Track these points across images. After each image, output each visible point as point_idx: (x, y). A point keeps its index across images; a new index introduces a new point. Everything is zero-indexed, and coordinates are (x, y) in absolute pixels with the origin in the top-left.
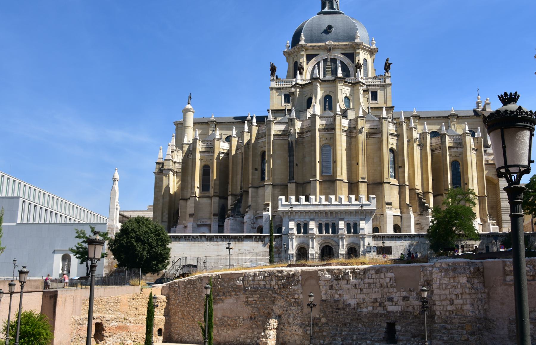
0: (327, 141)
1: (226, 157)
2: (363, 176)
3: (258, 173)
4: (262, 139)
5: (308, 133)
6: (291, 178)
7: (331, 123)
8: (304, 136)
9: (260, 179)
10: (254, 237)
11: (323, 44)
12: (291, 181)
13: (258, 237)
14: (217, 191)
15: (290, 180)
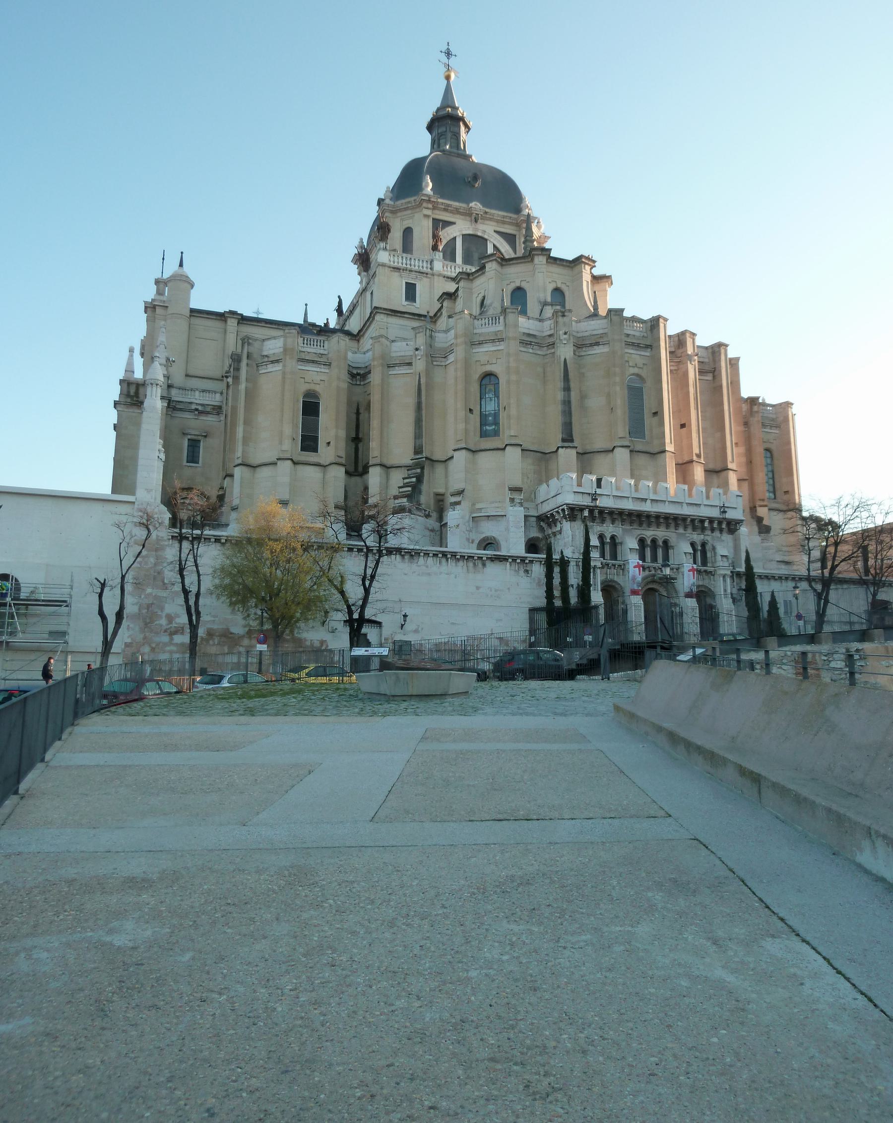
0: (636, 370)
1: (349, 380)
2: (698, 452)
3: (475, 418)
4: (485, 345)
5: (596, 347)
6: (568, 438)
7: (642, 334)
8: (583, 354)
9: (478, 434)
10: (510, 560)
11: (464, 205)
12: (566, 444)
13: (518, 561)
14: (342, 453)
15: (564, 440)
